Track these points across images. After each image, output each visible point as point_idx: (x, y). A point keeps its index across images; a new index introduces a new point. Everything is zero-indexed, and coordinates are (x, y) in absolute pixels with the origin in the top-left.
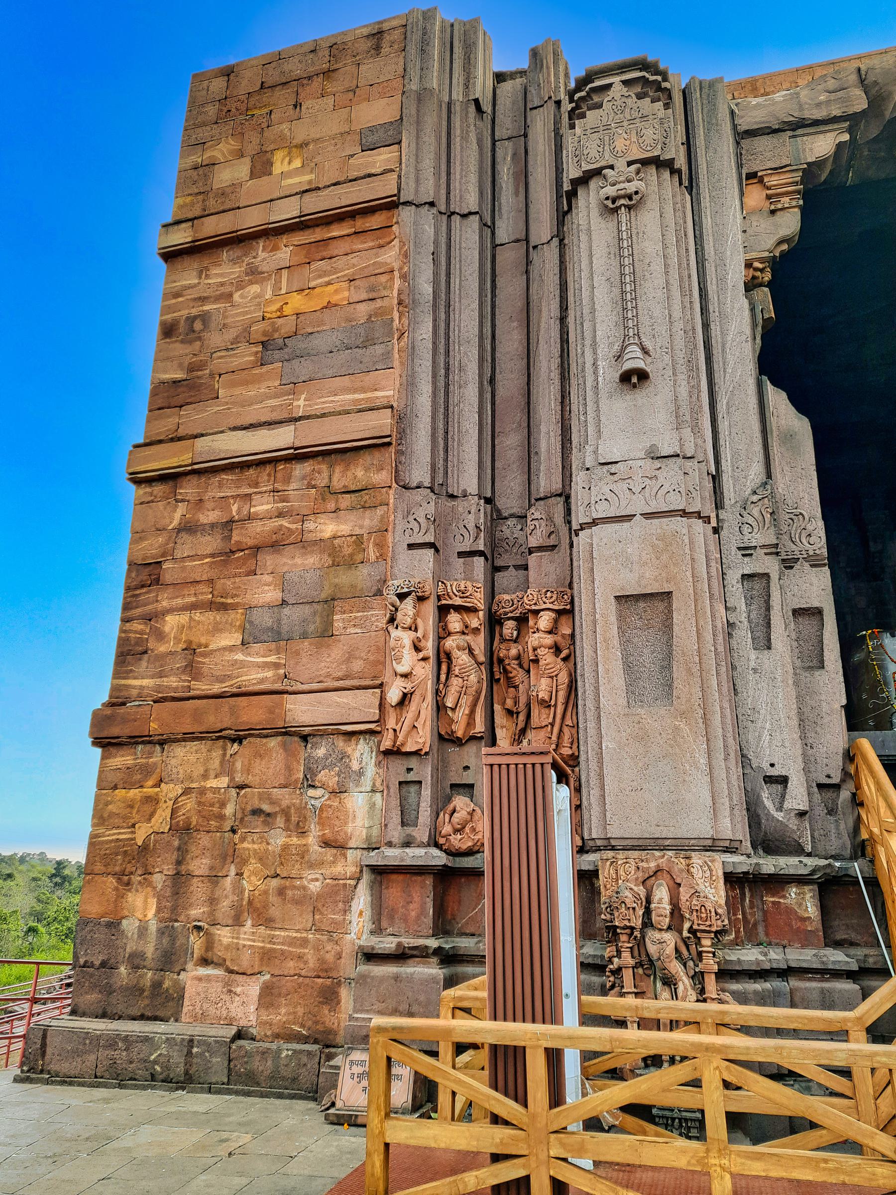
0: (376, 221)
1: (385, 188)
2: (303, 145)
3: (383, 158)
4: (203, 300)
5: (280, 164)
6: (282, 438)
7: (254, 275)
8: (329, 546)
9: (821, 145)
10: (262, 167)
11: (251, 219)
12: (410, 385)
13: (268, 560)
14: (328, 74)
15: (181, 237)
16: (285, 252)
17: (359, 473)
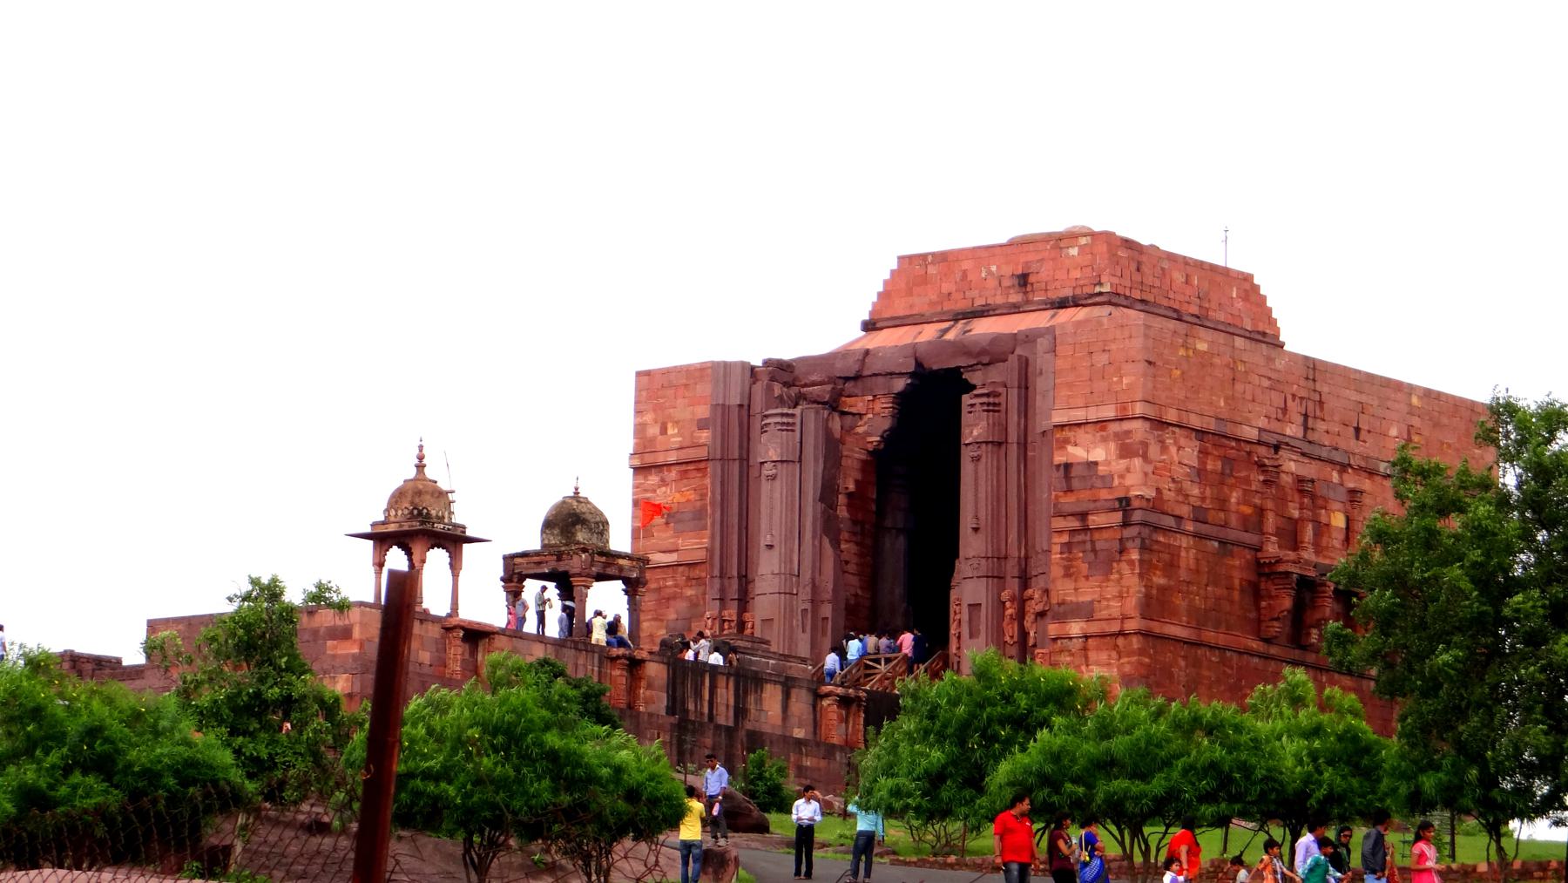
0: (702, 465)
1: (702, 453)
2: (677, 422)
3: (705, 436)
4: (646, 491)
5: (670, 431)
6: (671, 558)
7: (664, 483)
8: (689, 598)
9: (900, 384)
10: (664, 431)
11: (661, 459)
12: (713, 537)
13: (672, 602)
14: (686, 386)
15: (637, 463)
16: (673, 474)
17: (697, 572)
